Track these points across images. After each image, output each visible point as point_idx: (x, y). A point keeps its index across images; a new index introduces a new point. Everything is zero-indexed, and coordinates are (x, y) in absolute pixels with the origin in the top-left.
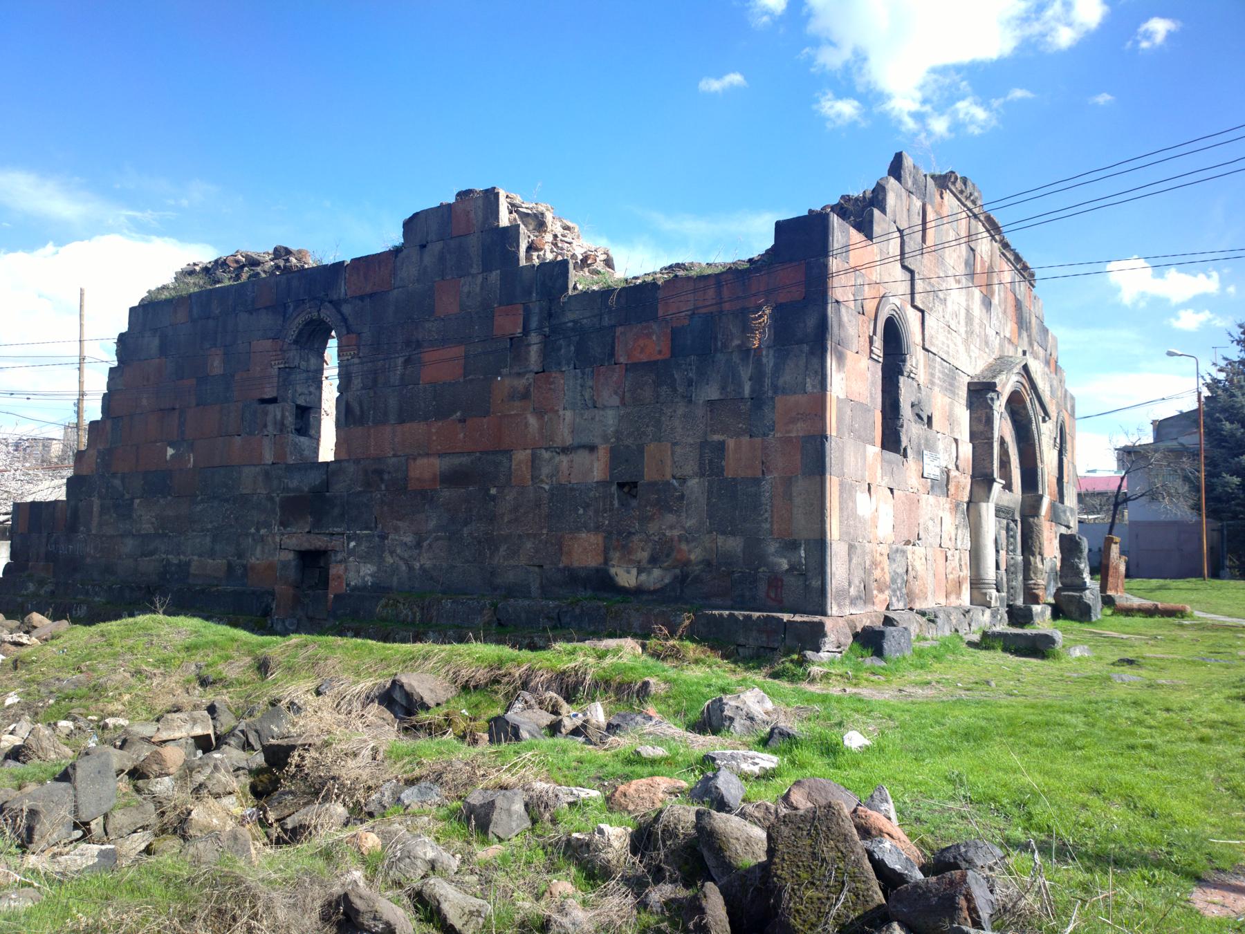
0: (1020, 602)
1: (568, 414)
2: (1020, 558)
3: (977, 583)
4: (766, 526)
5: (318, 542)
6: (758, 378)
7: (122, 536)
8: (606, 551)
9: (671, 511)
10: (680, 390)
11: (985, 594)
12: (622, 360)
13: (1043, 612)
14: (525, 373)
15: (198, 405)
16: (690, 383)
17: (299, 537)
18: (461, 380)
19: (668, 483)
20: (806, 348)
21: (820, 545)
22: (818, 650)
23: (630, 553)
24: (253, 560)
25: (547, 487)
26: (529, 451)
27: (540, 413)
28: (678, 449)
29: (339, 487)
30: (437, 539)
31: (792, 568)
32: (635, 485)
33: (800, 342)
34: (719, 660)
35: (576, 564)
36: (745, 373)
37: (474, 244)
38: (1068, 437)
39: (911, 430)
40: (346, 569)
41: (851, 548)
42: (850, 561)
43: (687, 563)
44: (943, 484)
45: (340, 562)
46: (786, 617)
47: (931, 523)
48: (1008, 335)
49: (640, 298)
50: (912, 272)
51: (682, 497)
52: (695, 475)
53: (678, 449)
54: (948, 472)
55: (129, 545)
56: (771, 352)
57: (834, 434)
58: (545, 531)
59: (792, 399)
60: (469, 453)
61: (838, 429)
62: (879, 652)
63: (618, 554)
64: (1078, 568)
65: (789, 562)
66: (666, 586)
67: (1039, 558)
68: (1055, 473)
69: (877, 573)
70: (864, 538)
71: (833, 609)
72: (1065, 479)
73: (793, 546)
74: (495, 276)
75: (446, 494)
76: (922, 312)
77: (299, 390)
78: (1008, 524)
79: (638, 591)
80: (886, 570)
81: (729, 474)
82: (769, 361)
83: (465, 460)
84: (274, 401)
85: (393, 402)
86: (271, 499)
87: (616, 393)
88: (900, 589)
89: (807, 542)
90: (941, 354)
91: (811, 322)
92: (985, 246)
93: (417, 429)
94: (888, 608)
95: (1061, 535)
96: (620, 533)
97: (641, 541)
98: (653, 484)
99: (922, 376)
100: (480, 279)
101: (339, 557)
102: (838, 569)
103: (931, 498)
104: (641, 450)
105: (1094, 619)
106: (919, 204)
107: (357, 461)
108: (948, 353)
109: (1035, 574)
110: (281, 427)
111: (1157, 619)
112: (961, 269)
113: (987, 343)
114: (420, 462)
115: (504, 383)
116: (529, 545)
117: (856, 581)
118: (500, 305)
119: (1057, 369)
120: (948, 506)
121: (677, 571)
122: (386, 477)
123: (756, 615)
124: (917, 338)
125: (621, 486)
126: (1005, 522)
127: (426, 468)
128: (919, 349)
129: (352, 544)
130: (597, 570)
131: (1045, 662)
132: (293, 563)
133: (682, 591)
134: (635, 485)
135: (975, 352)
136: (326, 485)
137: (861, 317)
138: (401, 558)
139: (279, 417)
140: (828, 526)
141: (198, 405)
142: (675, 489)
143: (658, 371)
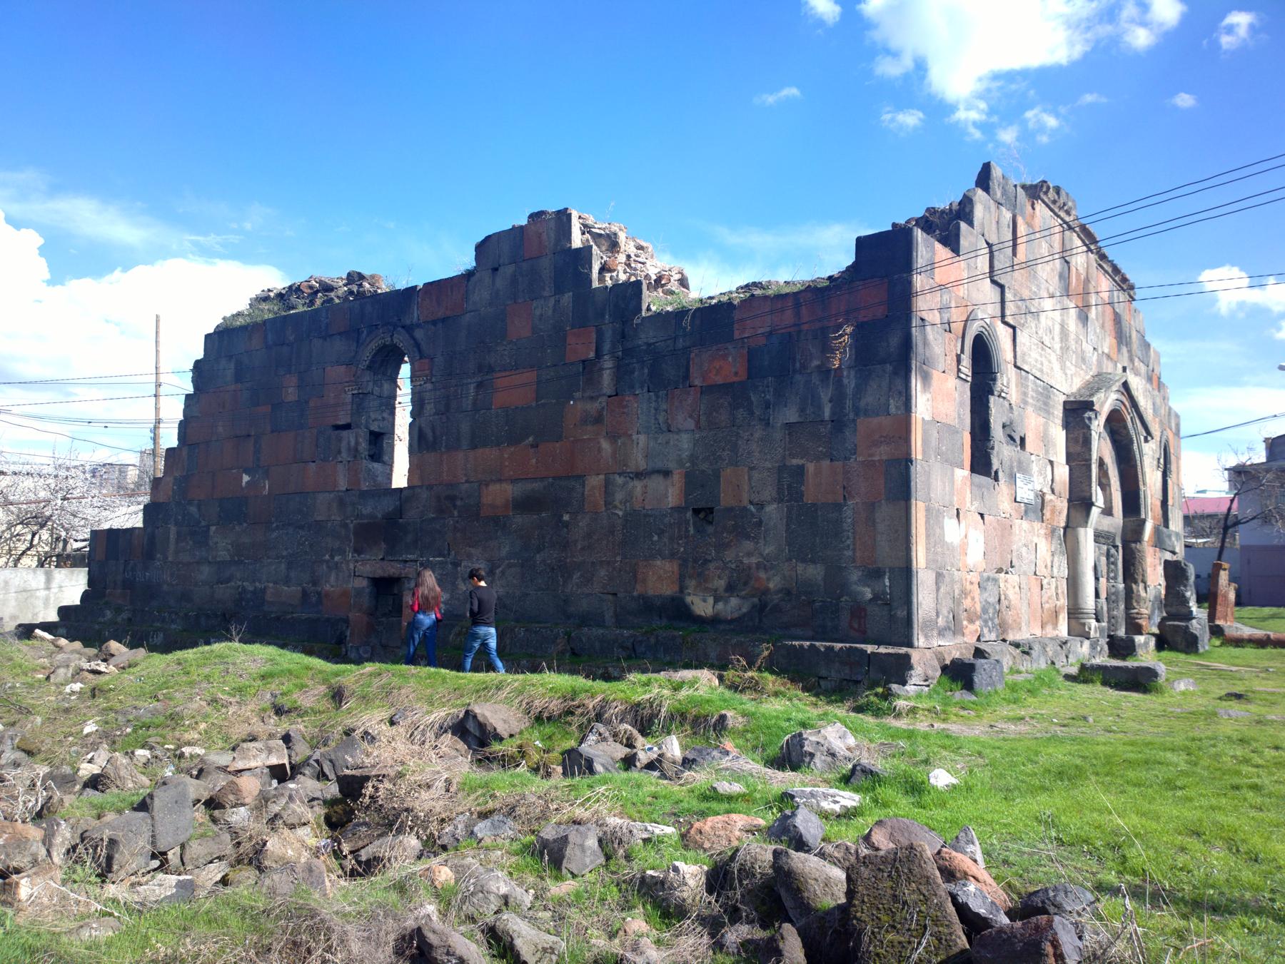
0: (1121, 632)
1: (642, 439)
2: (1121, 586)
3: (1075, 613)
4: (849, 553)
5: (392, 569)
6: (838, 400)
7: (198, 563)
8: (682, 578)
9: (748, 537)
10: (757, 413)
11: (1084, 624)
12: (697, 382)
13: (1146, 643)
14: (598, 397)
15: (272, 432)
16: (767, 405)
17: (374, 564)
18: (534, 404)
19: (745, 508)
20: (889, 368)
21: (905, 574)
22: (904, 683)
23: (706, 581)
24: (327, 587)
25: (620, 513)
26: (602, 477)
27: (613, 437)
28: (756, 475)
29: (412, 514)
30: (510, 566)
31: (876, 597)
32: (711, 510)
33: (883, 362)
34: (799, 693)
35: (651, 592)
36: (825, 395)
37: (546, 266)
38: (1173, 458)
39: (1002, 452)
41: (939, 576)
42: (938, 590)
43: (766, 591)
44: (1037, 509)
46: (870, 648)
47: (1024, 550)
48: (1106, 351)
49: (716, 316)
50: (1002, 287)
51: (760, 523)
52: (774, 500)
53: (756, 475)
54: (1043, 496)
55: (205, 572)
56: (853, 373)
57: (920, 457)
58: (618, 558)
59: (875, 421)
60: (542, 479)
61: (924, 452)
62: (969, 686)
63: (693, 583)
64: (1184, 596)
65: (873, 591)
66: (744, 615)
67: (1141, 585)
68: (1159, 495)
69: (967, 603)
70: (952, 565)
71: (920, 641)
72: (1170, 502)
73: (876, 574)
74: (567, 298)
75: (519, 520)
76: (1014, 328)
77: (373, 416)
78: (1108, 551)
79: (714, 621)
80: (977, 600)
81: (809, 498)
82: (850, 382)
83: (536, 486)
84: (347, 427)
85: (465, 427)
86: (345, 526)
87: (691, 416)
88: (992, 620)
89: (892, 570)
90: (1034, 371)
91: (895, 341)
92: (1081, 260)
93: (489, 454)
94: (979, 640)
95: (1166, 562)
96: (695, 561)
97: (717, 568)
98: (730, 510)
99: (1013, 395)
100: (552, 302)
102: (925, 599)
103: (1025, 524)
104: (717, 475)
105: (1201, 650)
106: (1007, 215)
107: (430, 487)
108: (1041, 371)
109: (1138, 602)
110: (355, 452)
111: (1269, 650)
112: (1055, 285)
113: (1083, 360)
114: (494, 488)
115: (577, 407)
116: (603, 573)
117: (944, 611)
118: (573, 327)
119: (1160, 386)
120: (1043, 532)
121: (756, 600)
122: (459, 503)
123: (838, 646)
124: (1009, 356)
125: (696, 512)
126: (1105, 547)
127: (499, 494)
128: (1011, 367)
130: (673, 599)
131: (1147, 697)
132: (367, 590)
133: (760, 620)
134: (711, 510)
135: (1071, 369)
136: (400, 512)
137: (947, 334)
139: (353, 443)
140: (914, 554)
141: (272, 432)
142: (753, 515)
143: (735, 393)
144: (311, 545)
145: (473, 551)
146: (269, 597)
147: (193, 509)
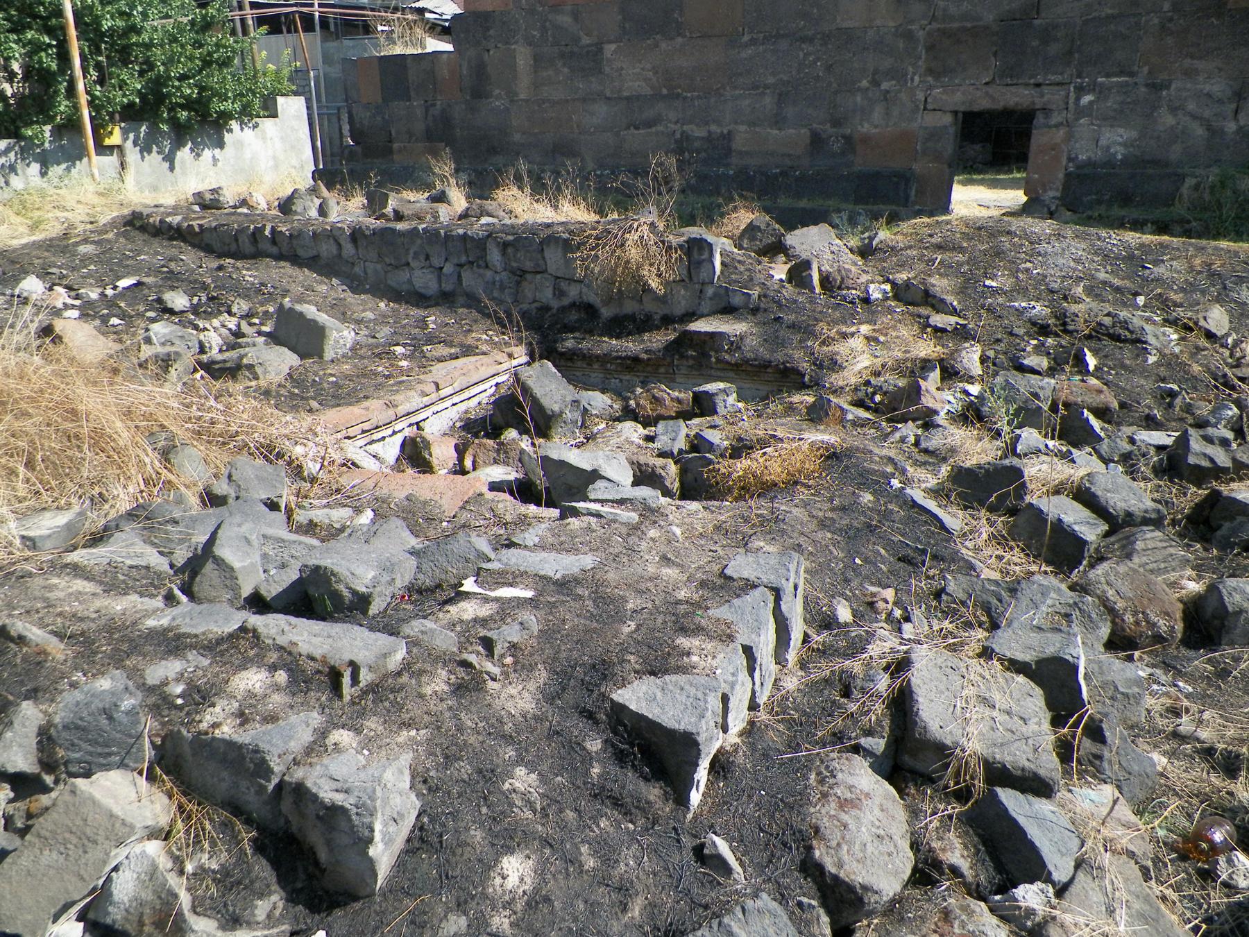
7: (584, 100)
24: (866, 128)
40: (1069, 137)
45: (1057, 126)
86: (909, 36)
101: (1056, 118)
129: (1087, 99)
132: (952, 130)
138: (1194, 117)
144: (829, 68)
145: (1200, 65)
146: (738, 143)
147: (565, 20)
